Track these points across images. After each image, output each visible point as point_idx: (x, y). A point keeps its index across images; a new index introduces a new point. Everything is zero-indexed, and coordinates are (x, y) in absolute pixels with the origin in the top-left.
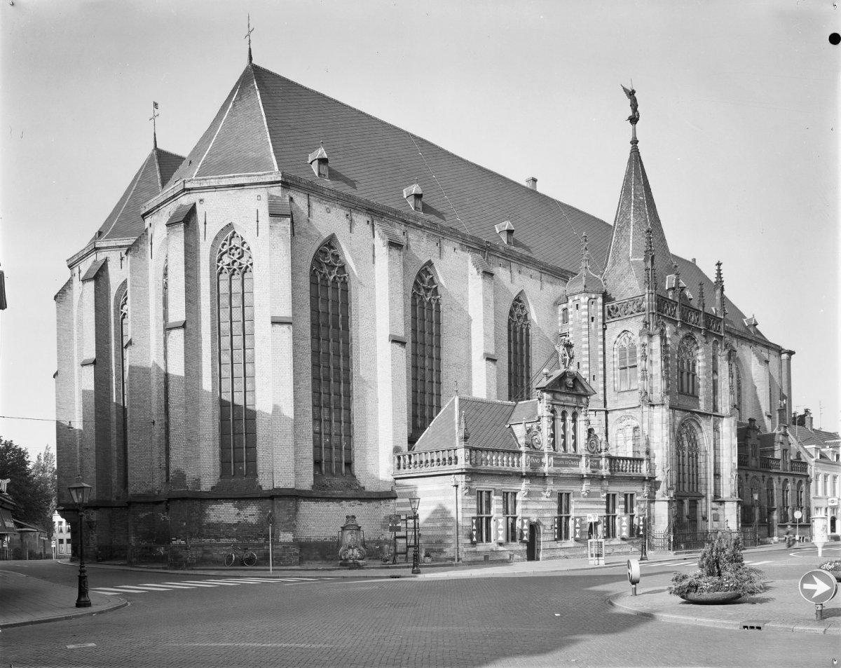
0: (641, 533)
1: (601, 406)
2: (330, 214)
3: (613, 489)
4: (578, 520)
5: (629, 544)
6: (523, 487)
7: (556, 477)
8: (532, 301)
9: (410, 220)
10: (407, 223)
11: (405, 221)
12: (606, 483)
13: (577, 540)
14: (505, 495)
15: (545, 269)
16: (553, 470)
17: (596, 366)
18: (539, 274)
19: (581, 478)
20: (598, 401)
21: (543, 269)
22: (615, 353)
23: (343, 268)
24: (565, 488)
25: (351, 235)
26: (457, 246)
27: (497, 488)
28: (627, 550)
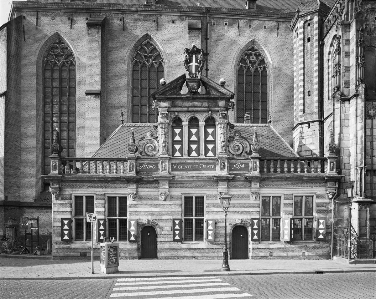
0: (321, 237)
1: (316, 117)
2: (54, 21)
3: (269, 191)
4: (210, 222)
5: (300, 248)
6: (128, 191)
7: (172, 182)
8: (267, 47)
9: (124, 8)
10: (123, 12)
11: (119, 11)
12: (255, 186)
13: (210, 242)
14: (111, 200)
15: (281, 18)
16: (166, 173)
17: (311, 82)
18: (276, 24)
19: (216, 180)
20: (313, 113)
21: (278, 18)
22: (330, 64)
23: (71, 55)
24: (195, 192)
25: (72, 30)
26: (175, 18)
27: (98, 193)
28: (295, 254)
